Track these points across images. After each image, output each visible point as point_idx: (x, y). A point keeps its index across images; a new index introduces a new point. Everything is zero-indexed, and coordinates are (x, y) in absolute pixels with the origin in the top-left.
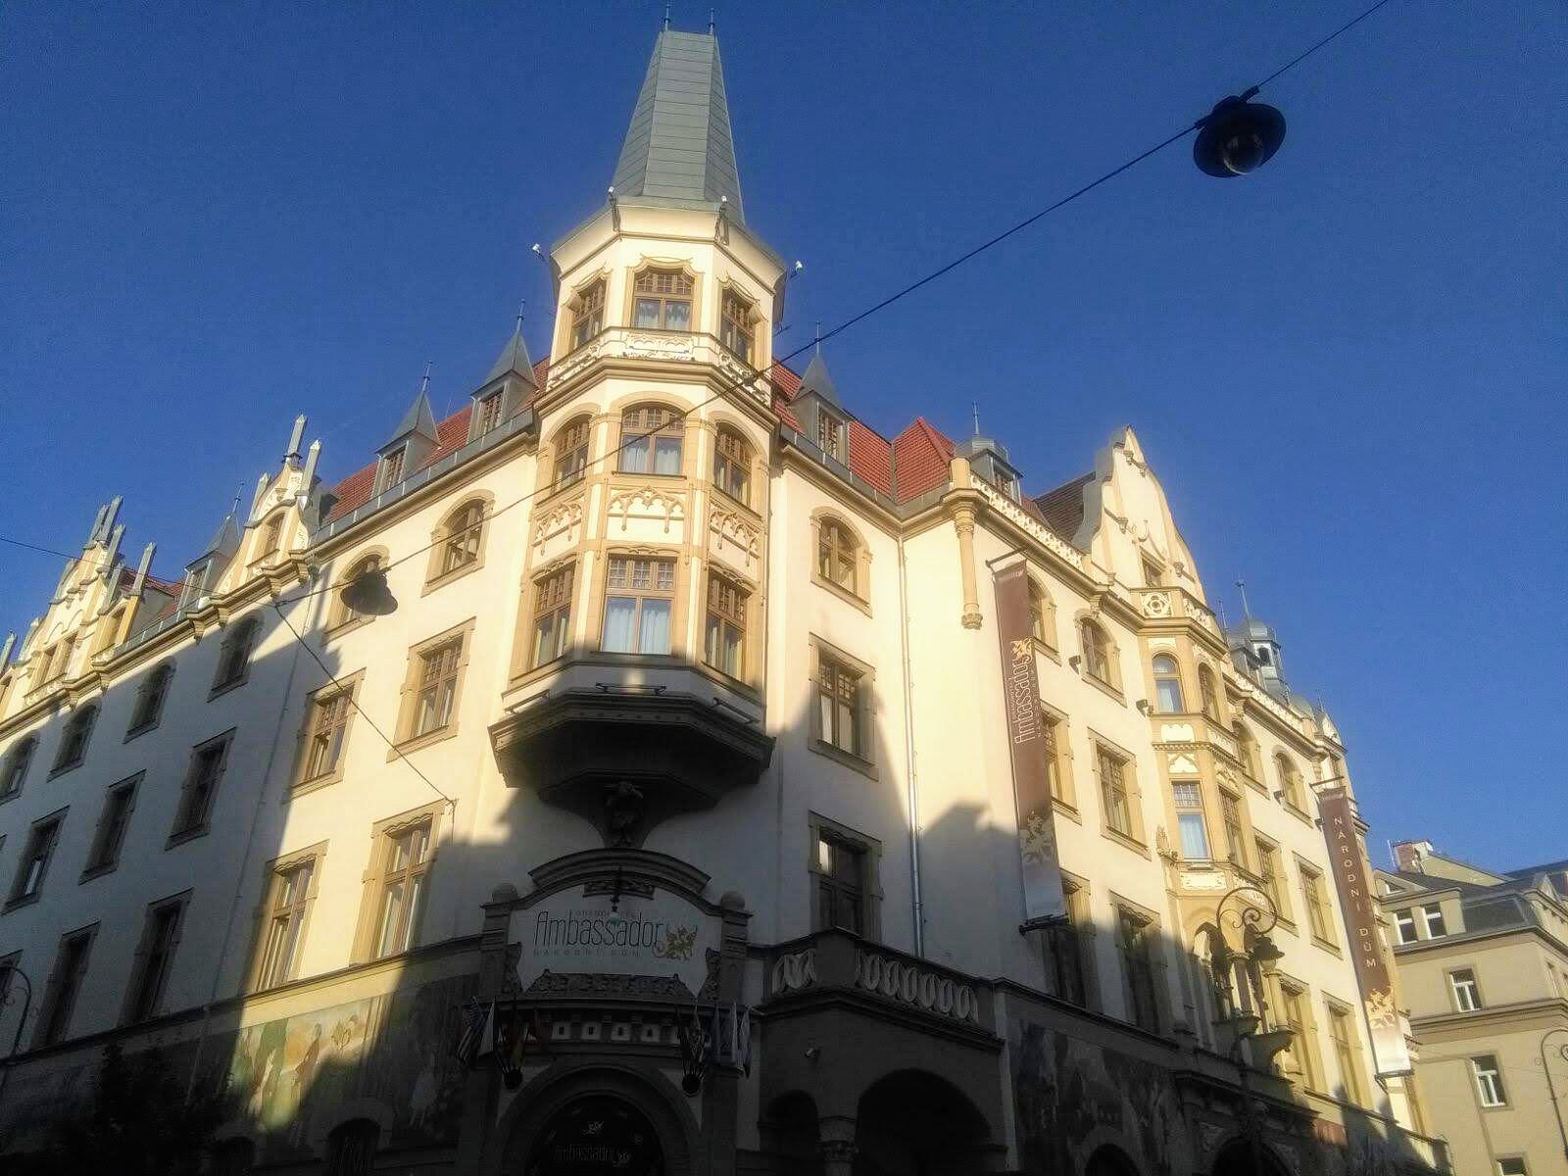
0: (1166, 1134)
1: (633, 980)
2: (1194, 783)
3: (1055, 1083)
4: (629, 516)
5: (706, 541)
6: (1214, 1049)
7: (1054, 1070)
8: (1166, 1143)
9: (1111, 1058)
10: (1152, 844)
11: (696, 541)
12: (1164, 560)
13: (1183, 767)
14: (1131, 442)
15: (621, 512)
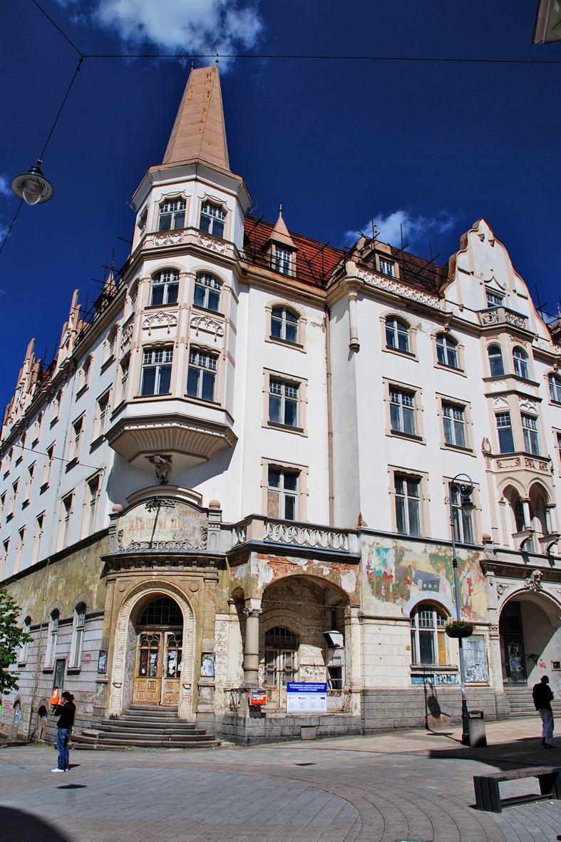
0: (470, 591)
1: (166, 543)
2: (507, 414)
3: (393, 574)
4: (152, 328)
5: (188, 333)
6: (512, 548)
7: (393, 568)
8: (470, 595)
9: (434, 557)
10: (478, 451)
11: (183, 334)
12: (504, 290)
13: (500, 405)
14: (483, 226)
15: (148, 326)
